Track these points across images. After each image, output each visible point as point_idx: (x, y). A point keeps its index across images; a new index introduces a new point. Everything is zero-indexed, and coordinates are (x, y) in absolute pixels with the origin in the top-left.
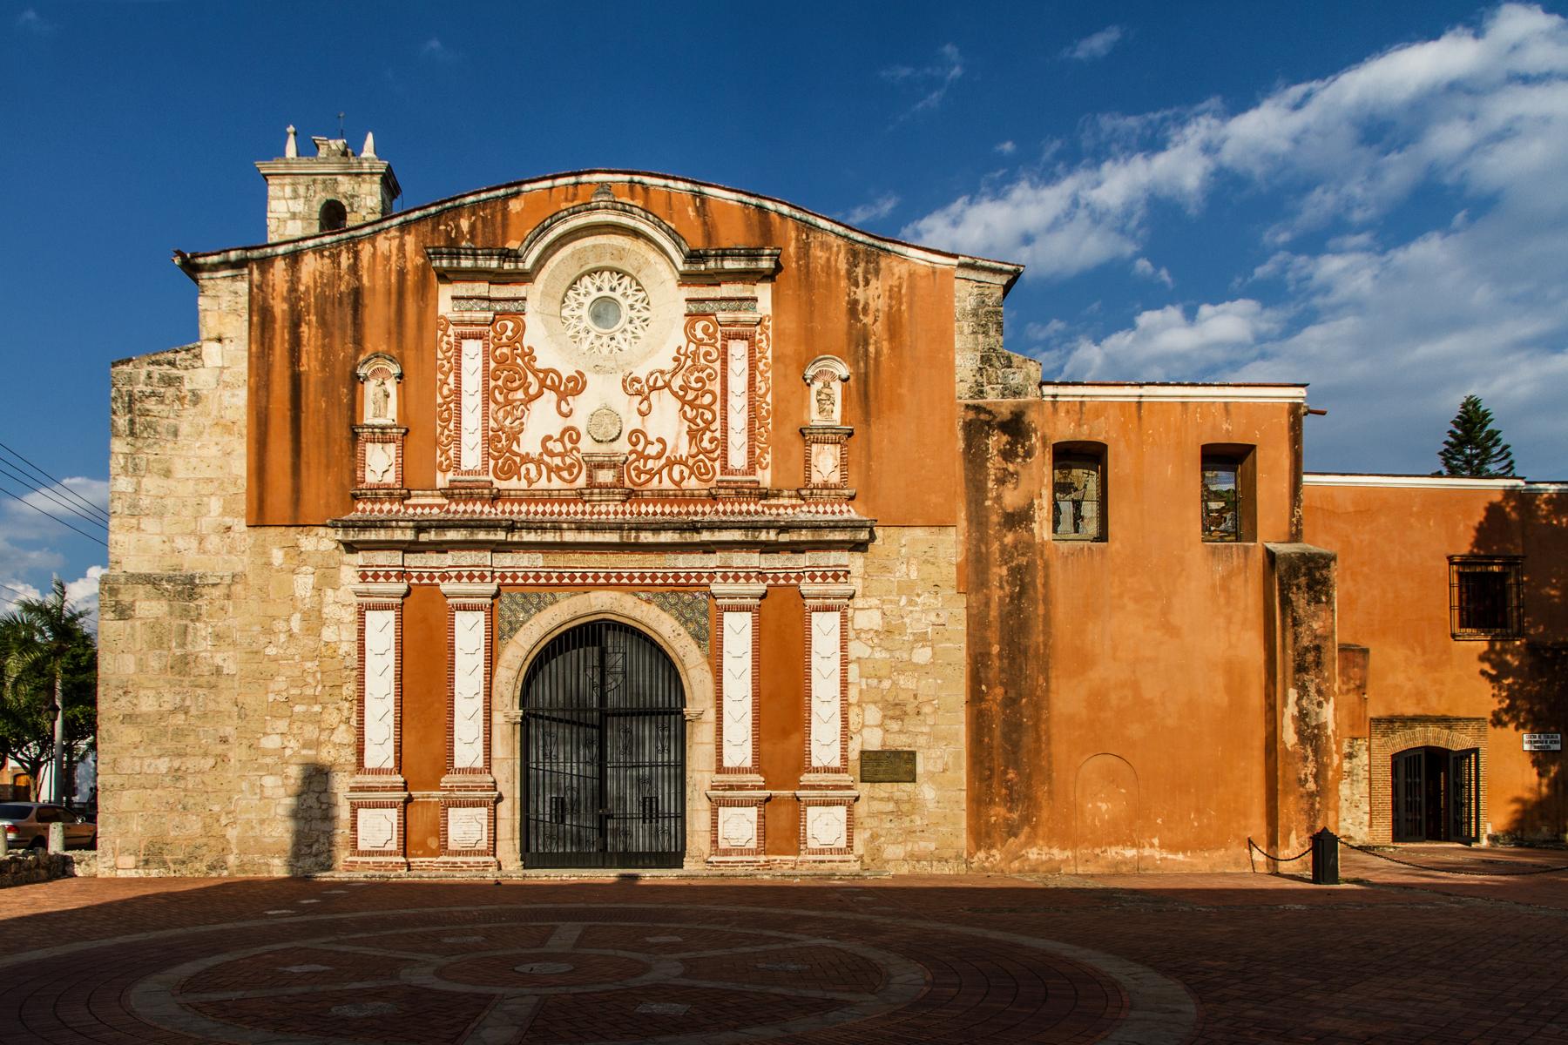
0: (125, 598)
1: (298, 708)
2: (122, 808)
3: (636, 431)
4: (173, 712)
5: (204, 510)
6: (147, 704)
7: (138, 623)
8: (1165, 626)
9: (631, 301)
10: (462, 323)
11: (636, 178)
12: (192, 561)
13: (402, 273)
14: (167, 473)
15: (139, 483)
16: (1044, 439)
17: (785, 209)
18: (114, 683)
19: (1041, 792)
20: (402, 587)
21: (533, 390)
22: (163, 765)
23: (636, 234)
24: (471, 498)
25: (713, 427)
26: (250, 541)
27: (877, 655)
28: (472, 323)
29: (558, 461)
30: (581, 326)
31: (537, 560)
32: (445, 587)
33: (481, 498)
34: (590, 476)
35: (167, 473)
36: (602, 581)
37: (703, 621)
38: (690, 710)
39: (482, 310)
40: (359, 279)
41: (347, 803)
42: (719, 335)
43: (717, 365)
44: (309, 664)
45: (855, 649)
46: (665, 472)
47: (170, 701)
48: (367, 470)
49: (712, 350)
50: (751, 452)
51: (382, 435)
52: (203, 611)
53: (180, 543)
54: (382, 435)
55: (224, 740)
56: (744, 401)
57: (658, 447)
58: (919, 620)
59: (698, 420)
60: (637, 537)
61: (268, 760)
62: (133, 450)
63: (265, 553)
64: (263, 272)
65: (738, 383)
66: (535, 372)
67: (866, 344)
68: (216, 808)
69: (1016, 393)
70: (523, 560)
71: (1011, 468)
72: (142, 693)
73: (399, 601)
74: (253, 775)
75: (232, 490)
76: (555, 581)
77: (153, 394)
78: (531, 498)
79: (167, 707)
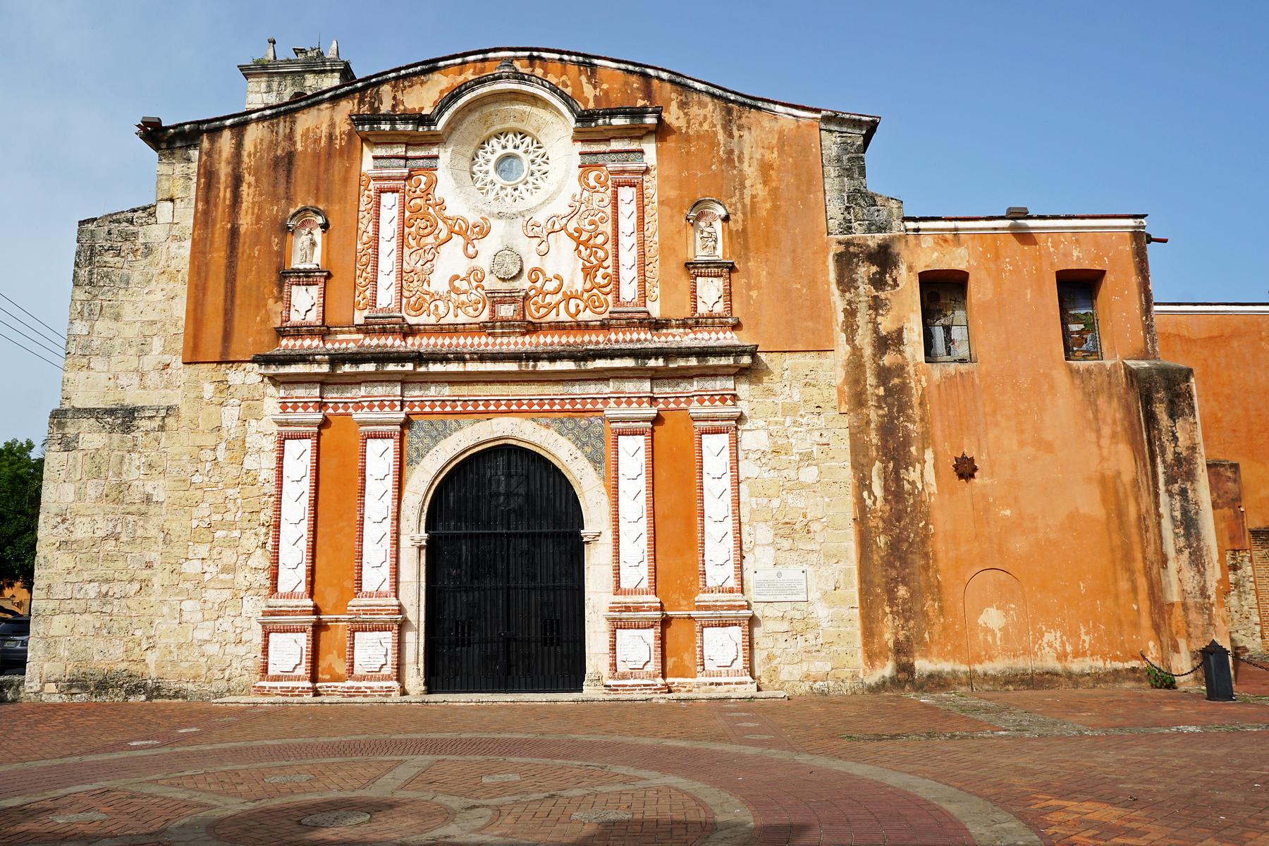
0: (71, 431)
1: (219, 534)
2: (52, 633)
3: (535, 270)
4: (105, 539)
5: (146, 348)
6: (82, 531)
8: (1039, 445)
9: (532, 156)
11: (535, 54)
12: (132, 398)
13: (331, 137)
14: (117, 317)
15: (92, 327)
16: (910, 268)
17: (665, 75)
18: (54, 510)
19: (930, 606)
20: (319, 417)
21: (443, 236)
22: (92, 590)
23: (534, 100)
24: (384, 331)
25: (605, 264)
26: (185, 377)
27: (766, 475)
28: (389, 178)
29: (463, 297)
30: (488, 179)
31: (447, 391)
32: (358, 416)
33: (393, 332)
34: (493, 311)
35: (117, 317)
36: (503, 408)
37: (599, 445)
38: (588, 531)
39: (400, 167)
40: (294, 144)
41: (260, 626)
42: (609, 183)
43: (609, 210)
44: (230, 492)
45: (746, 469)
46: (562, 305)
47: (103, 528)
48: (292, 309)
49: (603, 195)
51: (306, 277)
52: (139, 442)
53: (123, 381)
54: (306, 277)
55: (149, 566)
56: (634, 239)
57: (555, 283)
58: (803, 442)
59: (592, 258)
60: (535, 366)
61: (188, 585)
62: (90, 297)
63: (197, 385)
64: (212, 142)
65: (627, 224)
66: (445, 220)
67: (742, 186)
68: (138, 633)
69: (881, 229)
70: (433, 391)
71: (882, 295)
72: (77, 521)
73: (316, 429)
74: (174, 600)
75: (173, 330)
76: (459, 409)
77: (111, 248)
78: (440, 330)
79: (100, 533)
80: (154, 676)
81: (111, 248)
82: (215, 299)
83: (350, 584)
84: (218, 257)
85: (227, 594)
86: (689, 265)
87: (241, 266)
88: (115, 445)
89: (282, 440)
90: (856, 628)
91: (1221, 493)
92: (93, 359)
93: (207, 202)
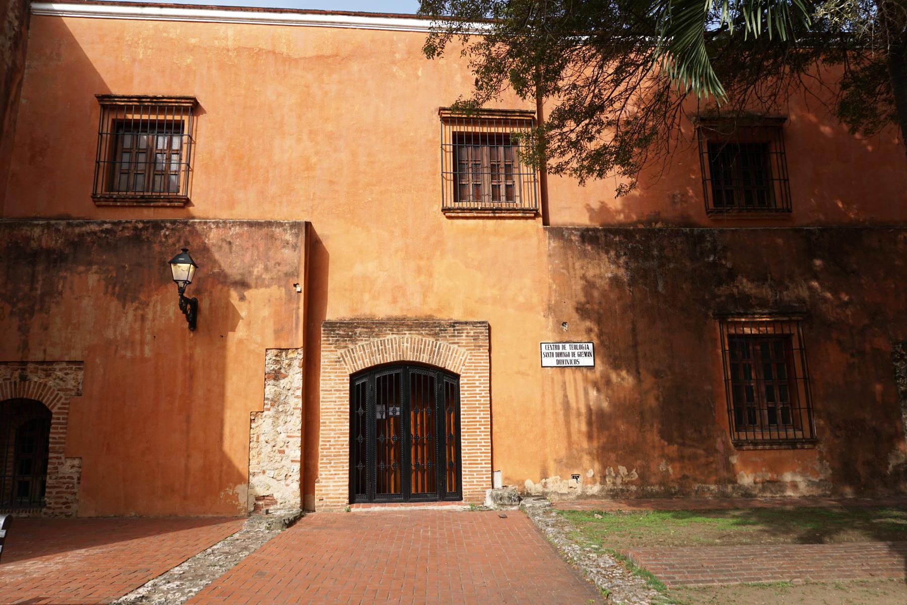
91: (271, 264)
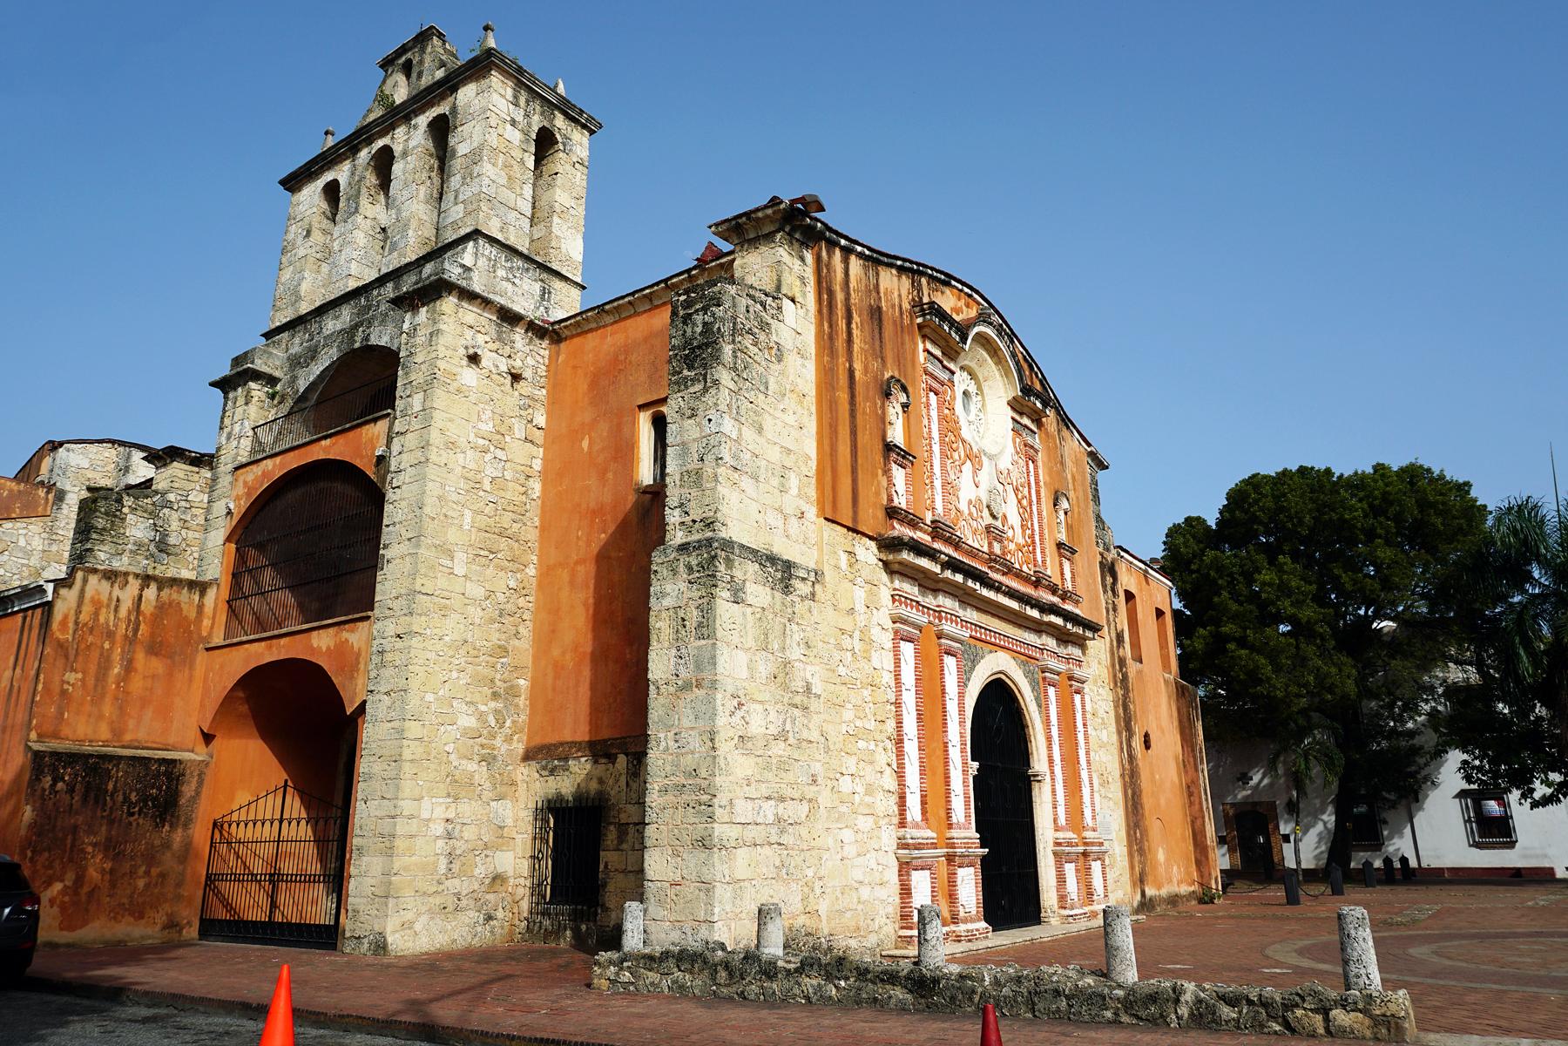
1: (862, 744)
6: (757, 726)
7: (749, 610)
10: (931, 375)
14: (760, 430)
22: (769, 809)
23: (994, 352)
44: (866, 693)
50: (1043, 552)
54: (905, 456)
61: (843, 809)
66: (964, 441)
68: (810, 873)
79: (773, 730)
80: (826, 932)
81: (750, 332)
82: (844, 449)
83: (943, 814)
84: (843, 396)
85: (870, 819)
86: (1060, 545)
87: (859, 417)
88: (778, 606)
89: (900, 637)
90: (1126, 863)
92: (744, 478)
93: (831, 326)
